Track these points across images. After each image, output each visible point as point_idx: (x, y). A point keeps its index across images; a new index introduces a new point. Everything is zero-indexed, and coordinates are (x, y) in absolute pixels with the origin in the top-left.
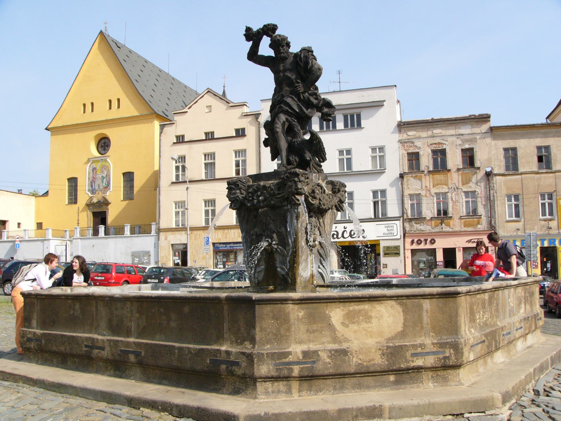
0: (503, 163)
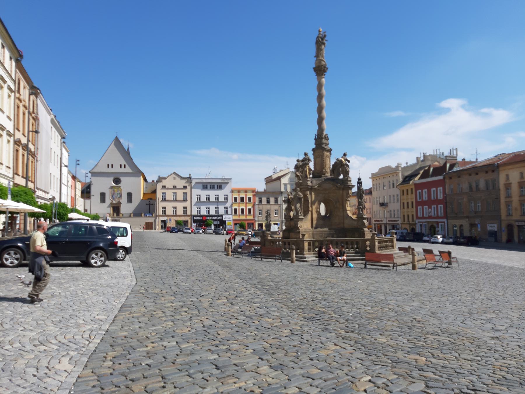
0: (258, 201)
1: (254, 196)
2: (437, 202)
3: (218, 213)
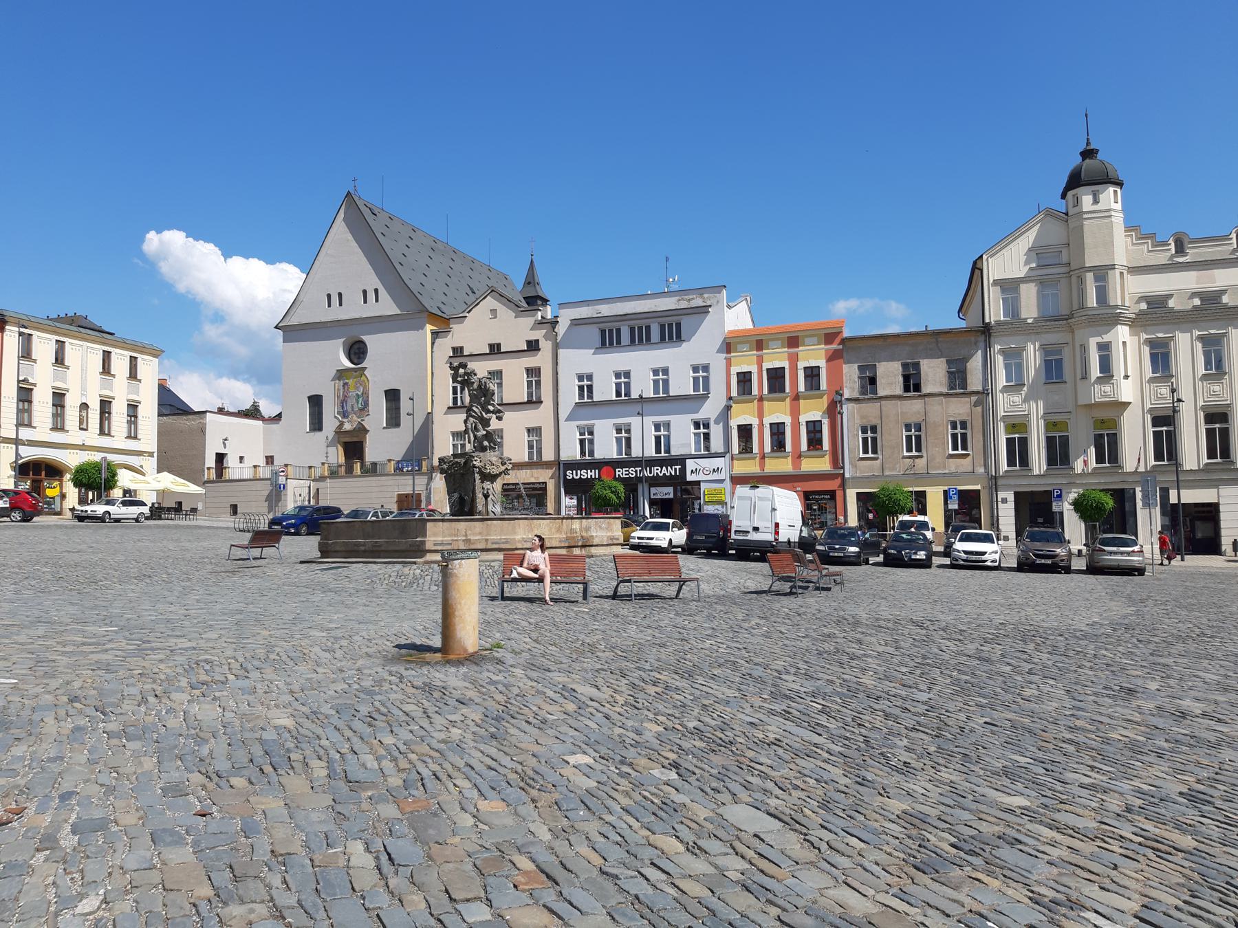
0: (857, 385)
1: (832, 357)
3: (668, 451)
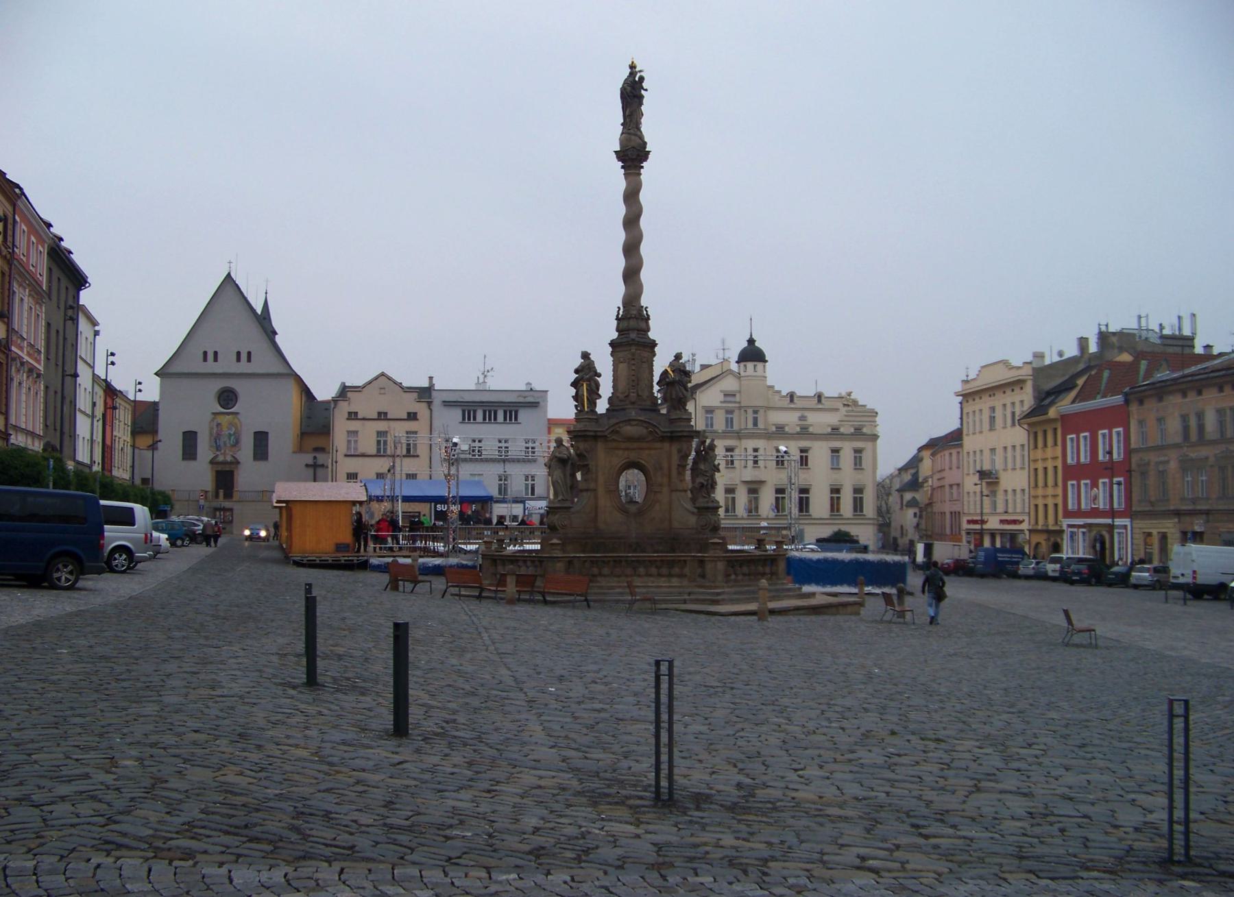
2: (1110, 469)
